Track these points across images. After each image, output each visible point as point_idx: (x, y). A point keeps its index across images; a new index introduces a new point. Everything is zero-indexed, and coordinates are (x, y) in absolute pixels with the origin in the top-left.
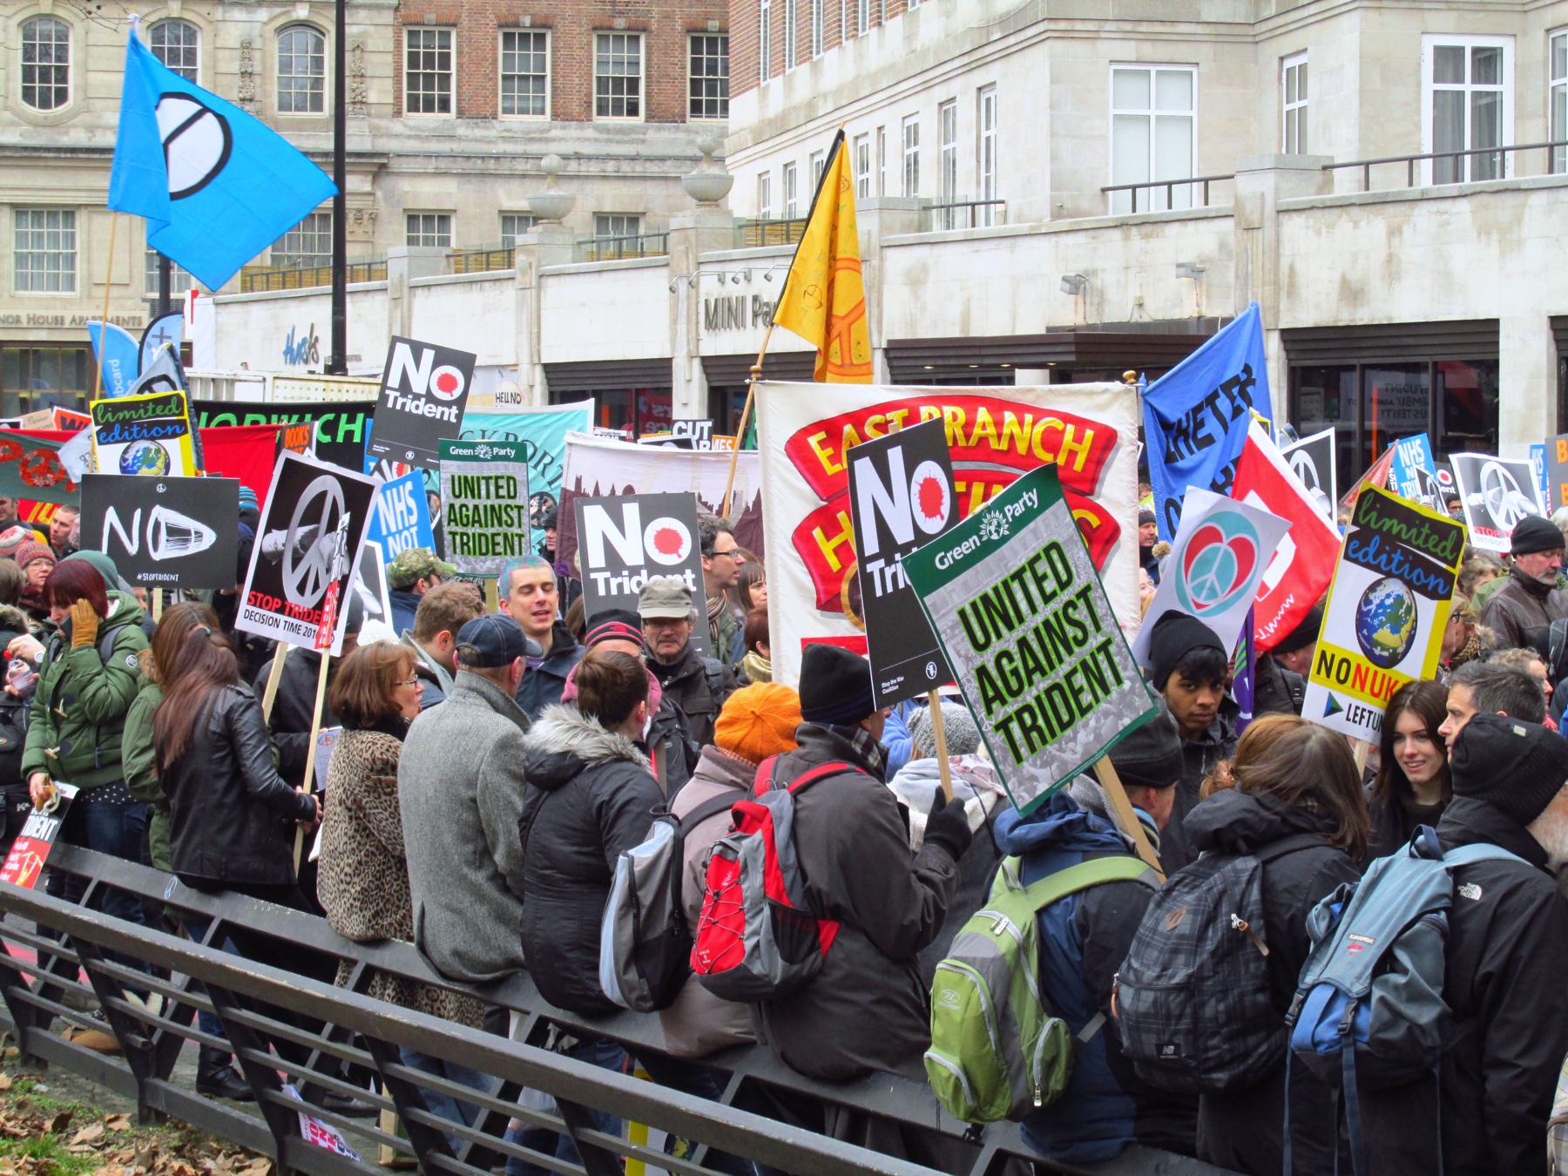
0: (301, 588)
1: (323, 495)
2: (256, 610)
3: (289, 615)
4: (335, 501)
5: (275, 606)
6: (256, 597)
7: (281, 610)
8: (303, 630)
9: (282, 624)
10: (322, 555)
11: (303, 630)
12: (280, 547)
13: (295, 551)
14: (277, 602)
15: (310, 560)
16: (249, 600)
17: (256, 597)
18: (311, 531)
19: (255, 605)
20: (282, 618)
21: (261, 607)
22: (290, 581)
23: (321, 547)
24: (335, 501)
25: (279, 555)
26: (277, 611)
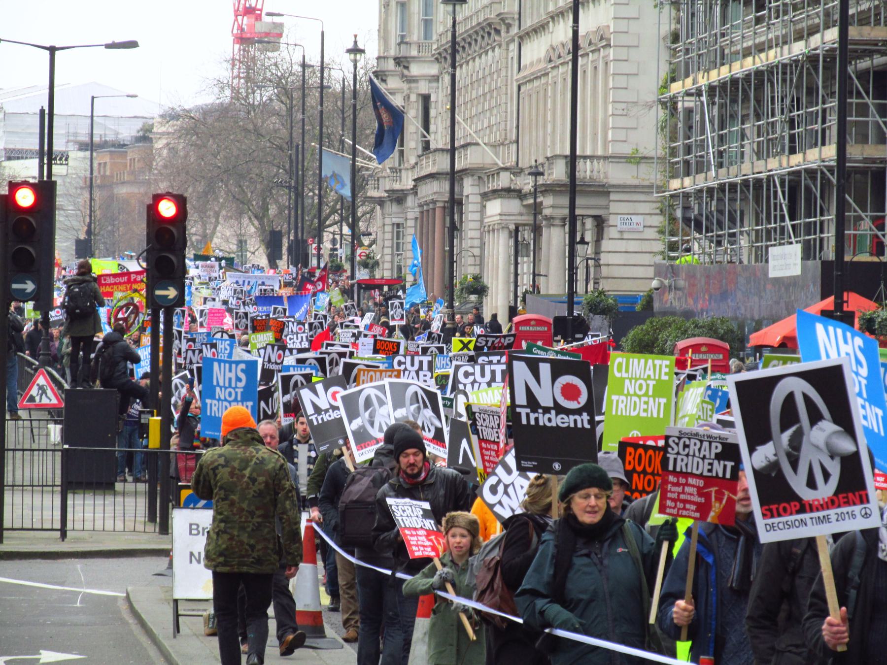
0: (811, 483)
1: (790, 398)
2: (776, 520)
3: (811, 511)
4: (806, 398)
5: (794, 509)
6: (771, 511)
8: (833, 517)
9: (809, 522)
10: (817, 447)
11: (833, 517)
12: (773, 458)
13: (789, 455)
14: (795, 505)
15: (807, 456)
16: (764, 516)
17: (771, 511)
18: (795, 432)
19: (772, 516)
21: (779, 515)
22: (797, 483)
23: (813, 440)
24: (806, 398)
25: (775, 466)
26: (799, 512)
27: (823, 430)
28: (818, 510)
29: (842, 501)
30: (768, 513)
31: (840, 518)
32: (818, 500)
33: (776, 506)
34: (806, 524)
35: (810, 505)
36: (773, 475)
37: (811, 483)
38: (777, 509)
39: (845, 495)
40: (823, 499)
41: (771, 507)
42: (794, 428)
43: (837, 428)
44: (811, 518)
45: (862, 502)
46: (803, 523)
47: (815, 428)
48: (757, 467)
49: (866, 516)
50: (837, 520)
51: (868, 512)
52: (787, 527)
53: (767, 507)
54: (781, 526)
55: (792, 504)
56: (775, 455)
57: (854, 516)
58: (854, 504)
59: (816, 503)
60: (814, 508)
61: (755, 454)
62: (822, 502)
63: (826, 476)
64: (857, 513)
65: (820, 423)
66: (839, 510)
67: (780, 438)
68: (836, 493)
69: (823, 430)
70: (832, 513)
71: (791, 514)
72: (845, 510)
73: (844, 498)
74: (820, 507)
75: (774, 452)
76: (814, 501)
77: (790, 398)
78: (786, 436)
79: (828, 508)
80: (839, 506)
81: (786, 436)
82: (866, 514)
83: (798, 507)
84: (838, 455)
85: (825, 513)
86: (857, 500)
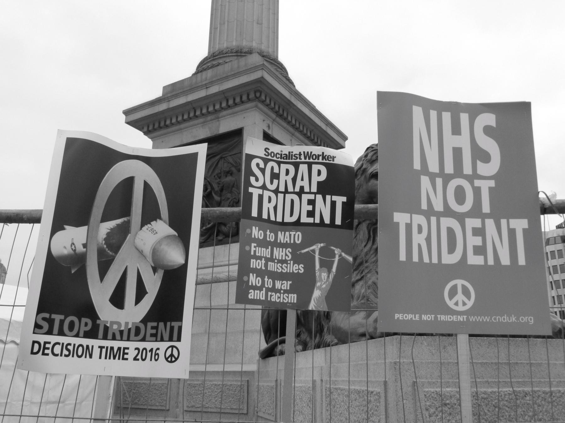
1: (129, 182)
2: (53, 339)
3: (105, 338)
5: (83, 329)
6: (51, 322)
7: (92, 334)
8: (132, 353)
9: (96, 352)
10: (141, 252)
11: (132, 353)
12: (80, 249)
13: (101, 252)
14: (86, 323)
18: (125, 221)
19: (50, 332)
20: (95, 343)
21: (61, 333)
23: (139, 242)
27: (154, 232)
28: (114, 338)
29: (150, 331)
30: (46, 326)
31: (141, 355)
32: (119, 324)
33: (62, 317)
34: (91, 356)
35: (106, 329)
36: (73, 272)
38: (62, 322)
39: (155, 324)
40: (127, 324)
41: (53, 316)
42: (119, 221)
43: (172, 232)
44: (101, 348)
45: (171, 340)
46: (88, 352)
47: (145, 228)
48: (56, 252)
49: (172, 359)
50: (135, 359)
51: (175, 353)
52: (65, 352)
53: (47, 315)
54: (57, 349)
55: (84, 320)
56: (85, 246)
57: (156, 356)
58: (162, 340)
59: (115, 327)
60: (110, 336)
61: (59, 235)
62: (122, 328)
64: (161, 353)
65: (153, 223)
66: (141, 345)
67: (98, 227)
68: (145, 321)
69: (154, 232)
70: (132, 346)
71: (77, 336)
72: (148, 345)
73: (153, 328)
74: (118, 336)
75: (84, 241)
76: (112, 323)
77: (129, 182)
78: (106, 227)
79: (128, 340)
80: (143, 340)
81: (106, 227)
82: (172, 355)
83: (89, 328)
84: (162, 267)
85: (123, 344)
86: (166, 336)
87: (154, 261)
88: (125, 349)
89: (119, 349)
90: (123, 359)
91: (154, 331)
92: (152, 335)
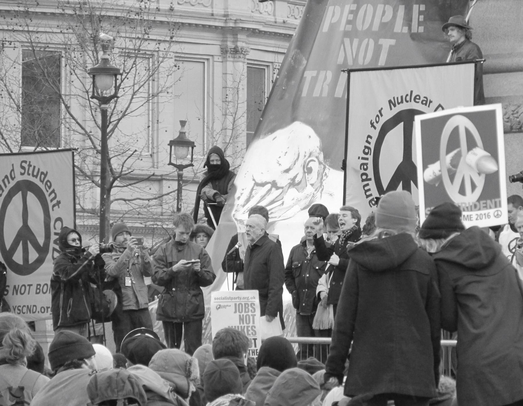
0: (462, 191)
1: (456, 130)
13: (449, 171)
15: (462, 172)
27: (475, 154)
29: (482, 205)
32: (465, 203)
37: (462, 191)
39: (485, 201)
42: (455, 152)
45: (496, 207)
49: (498, 216)
50: (477, 219)
51: (499, 213)
56: (440, 171)
57: (489, 216)
58: (491, 208)
59: (464, 205)
62: (467, 205)
63: (474, 187)
64: (491, 214)
66: (479, 212)
68: (479, 200)
69: (475, 154)
72: (483, 212)
76: (462, 203)
77: (456, 130)
78: (449, 157)
80: (480, 209)
82: (498, 215)
84: (484, 173)
87: (478, 170)
88: (470, 215)
89: (468, 216)
90: (471, 220)
91: (485, 205)
92: (484, 207)
